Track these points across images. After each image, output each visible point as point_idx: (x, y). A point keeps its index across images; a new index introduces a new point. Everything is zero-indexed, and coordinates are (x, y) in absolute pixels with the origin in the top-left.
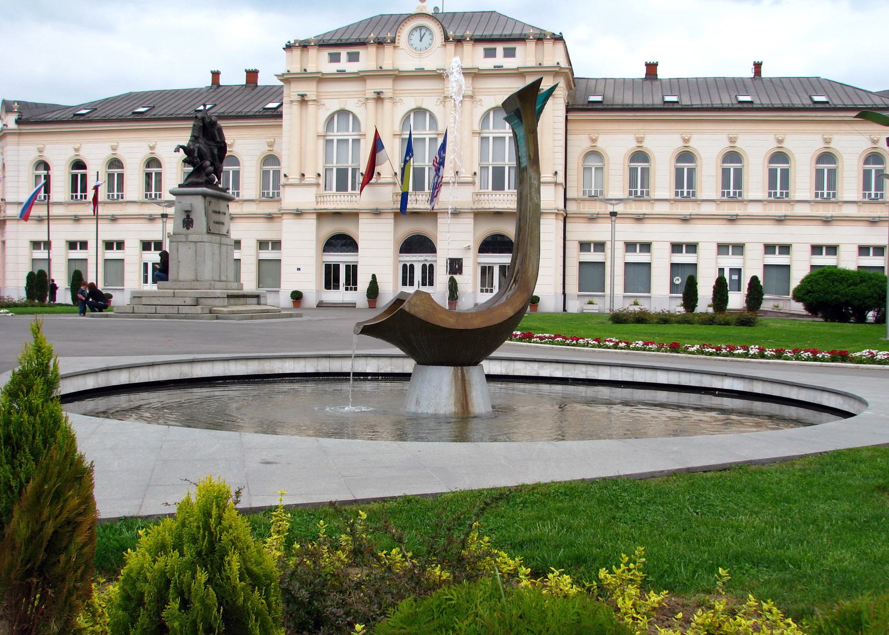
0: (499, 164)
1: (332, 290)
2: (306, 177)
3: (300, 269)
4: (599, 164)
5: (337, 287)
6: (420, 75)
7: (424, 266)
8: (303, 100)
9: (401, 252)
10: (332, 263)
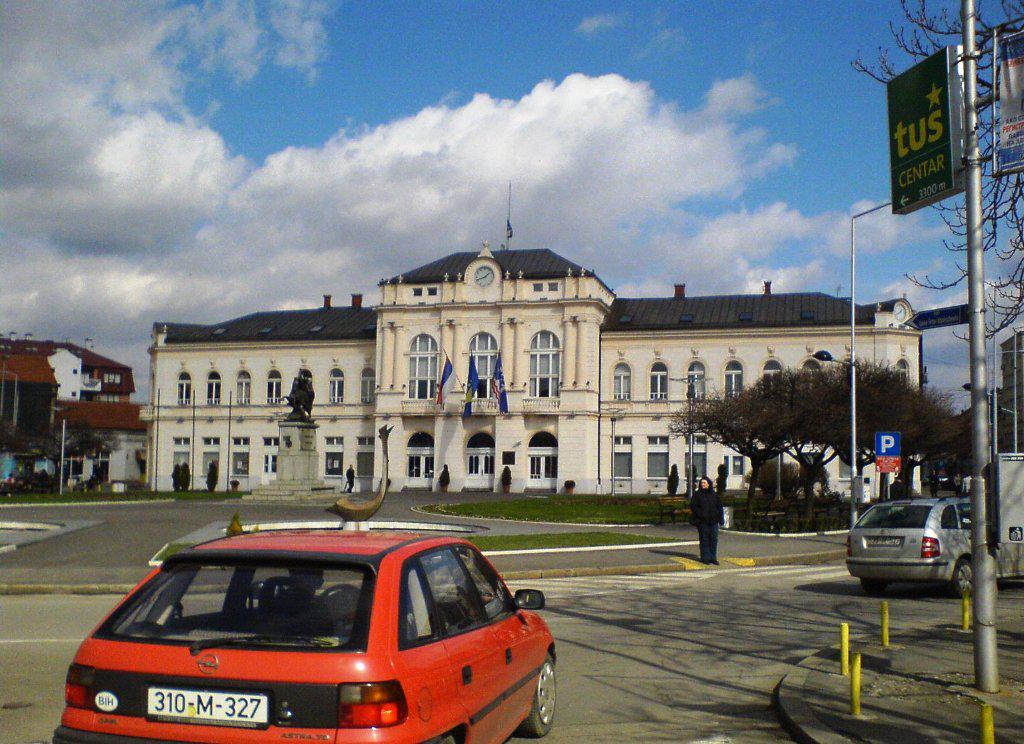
4: (627, 374)
5: (418, 475)
6: (482, 306)
7: (486, 458)
8: (392, 326)
9: (468, 446)
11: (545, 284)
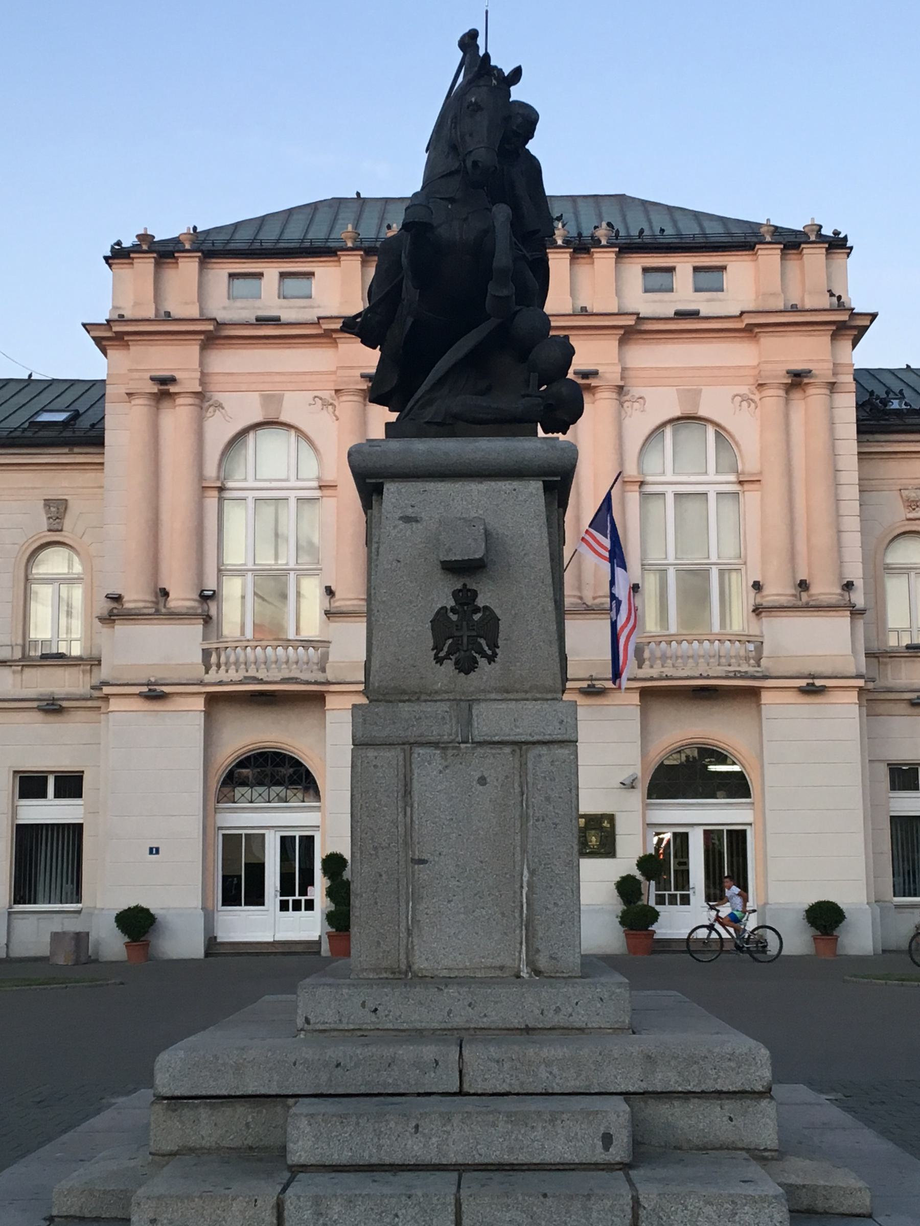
0: (694, 559)
1: (243, 908)
2: (172, 596)
3: (151, 852)
10: (243, 832)
11: (684, 265)
